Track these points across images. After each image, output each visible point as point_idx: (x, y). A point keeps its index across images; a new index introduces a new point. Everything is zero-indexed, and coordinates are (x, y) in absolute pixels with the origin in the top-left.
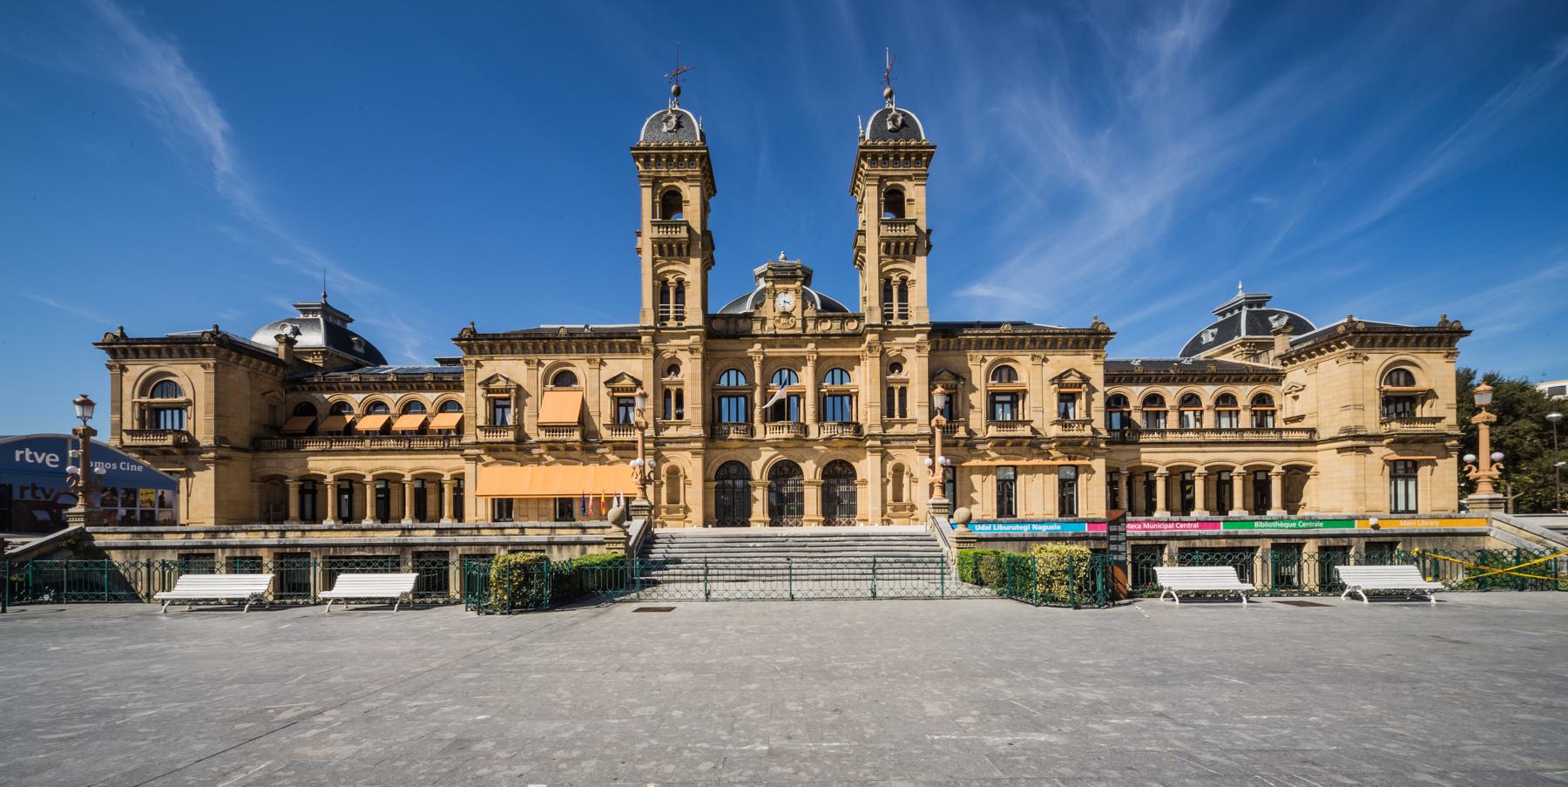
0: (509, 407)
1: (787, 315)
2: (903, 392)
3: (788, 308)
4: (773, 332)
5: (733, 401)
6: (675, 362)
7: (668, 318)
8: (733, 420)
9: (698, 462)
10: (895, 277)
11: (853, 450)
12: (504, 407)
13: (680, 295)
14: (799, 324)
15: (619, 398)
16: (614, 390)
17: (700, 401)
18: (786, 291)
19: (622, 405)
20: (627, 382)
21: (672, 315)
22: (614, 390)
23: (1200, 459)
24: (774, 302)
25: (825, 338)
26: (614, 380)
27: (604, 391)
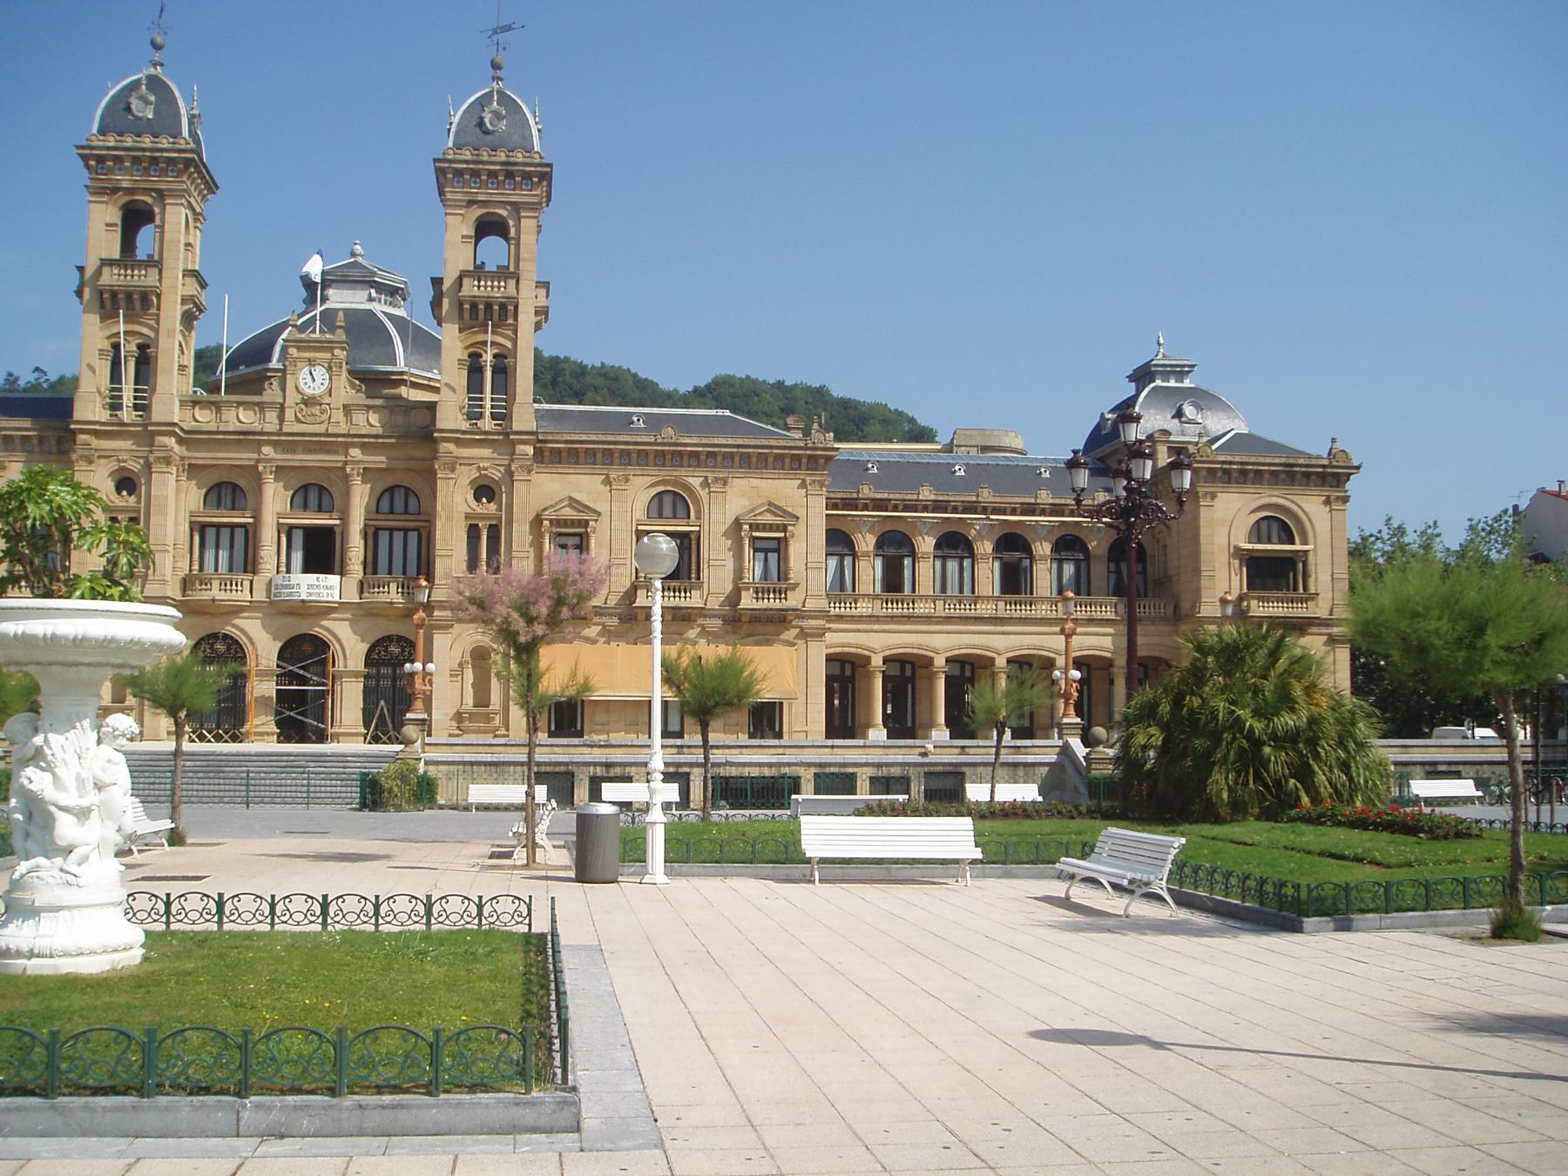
2: (494, 531)
6: (125, 474)
13: (143, 367)
14: (339, 416)
23: (941, 644)
24: (297, 379)
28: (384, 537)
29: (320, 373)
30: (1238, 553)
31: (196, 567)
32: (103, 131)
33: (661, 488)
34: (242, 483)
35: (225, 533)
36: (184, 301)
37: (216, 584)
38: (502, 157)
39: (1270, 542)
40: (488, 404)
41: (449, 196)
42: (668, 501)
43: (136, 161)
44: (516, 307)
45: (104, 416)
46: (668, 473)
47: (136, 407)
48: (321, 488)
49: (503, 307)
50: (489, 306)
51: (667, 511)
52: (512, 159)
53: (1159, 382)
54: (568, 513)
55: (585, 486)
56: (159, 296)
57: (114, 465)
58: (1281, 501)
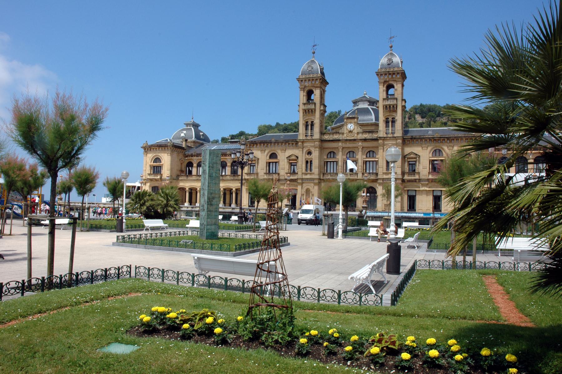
0: (255, 166)
3: (352, 129)
4: (346, 139)
5: (332, 163)
7: (308, 136)
8: (332, 172)
9: (316, 188)
10: (390, 119)
11: (375, 183)
12: (253, 166)
14: (356, 135)
15: (291, 163)
17: (318, 165)
18: (351, 123)
20: (293, 157)
21: (309, 134)
22: (290, 160)
25: (365, 140)
26: (289, 156)
27: (286, 160)
28: (368, 163)
31: (325, 171)
32: (302, 75)
33: (435, 149)
34: (335, 151)
35: (332, 163)
36: (321, 110)
38: (392, 70)
40: (390, 130)
42: (437, 151)
44: (397, 106)
45: (304, 138)
47: (311, 136)
48: (353, 152)
49: (393, 106)
50: (390, 106)
51: (438, 154)
54: (412, 156)
55: (417, 150)
56: (315, 110)
57: (307, 149)
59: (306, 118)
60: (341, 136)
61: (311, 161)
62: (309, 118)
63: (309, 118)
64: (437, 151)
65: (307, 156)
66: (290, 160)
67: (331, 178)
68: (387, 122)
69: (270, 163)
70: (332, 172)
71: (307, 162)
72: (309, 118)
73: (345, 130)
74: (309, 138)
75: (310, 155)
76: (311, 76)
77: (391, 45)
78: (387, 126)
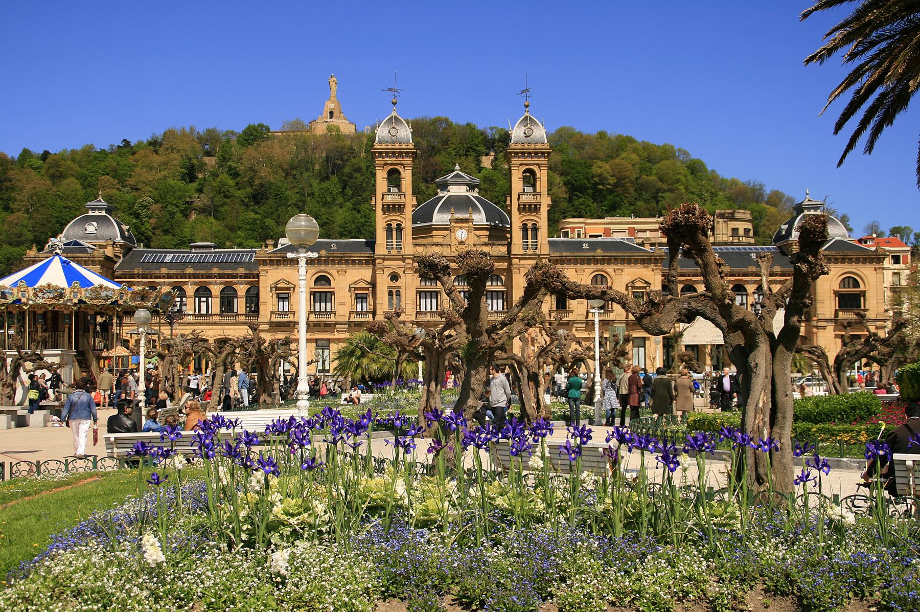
1: (461, 243)
3: (464, 238)
15: (357, 294)
16: (355, 289)
18: (461, 228)
19: (359, 298)
29: (465, 232)
30: (836, 293)
33: (596, 273)
37: (429, 315)
39: (849, 288)
41: (513, 163)
42: (599, 278)
43: (394, 153)
46: (599, 266)
52: (537, 147)
53: (806, 212)
57: (391, 271)
58: (853, 270)
59: (388, 219)
60: (445, 249)
61: (398, 294)
62: (394, 218)
63: (395, 218)
64: (599, 278)
65: (390, 282)
66: (355, 289)
67: (432, 319)
68: (525, 228)
69: (315, 292)
70: (429, 309)
71: (390, 293)
72: (394, 218)
73: (453, 239)
74: (394, 252)
75: (397, 281)
76: (397, 146)
77: (527, 104)
78: (525, 236)
